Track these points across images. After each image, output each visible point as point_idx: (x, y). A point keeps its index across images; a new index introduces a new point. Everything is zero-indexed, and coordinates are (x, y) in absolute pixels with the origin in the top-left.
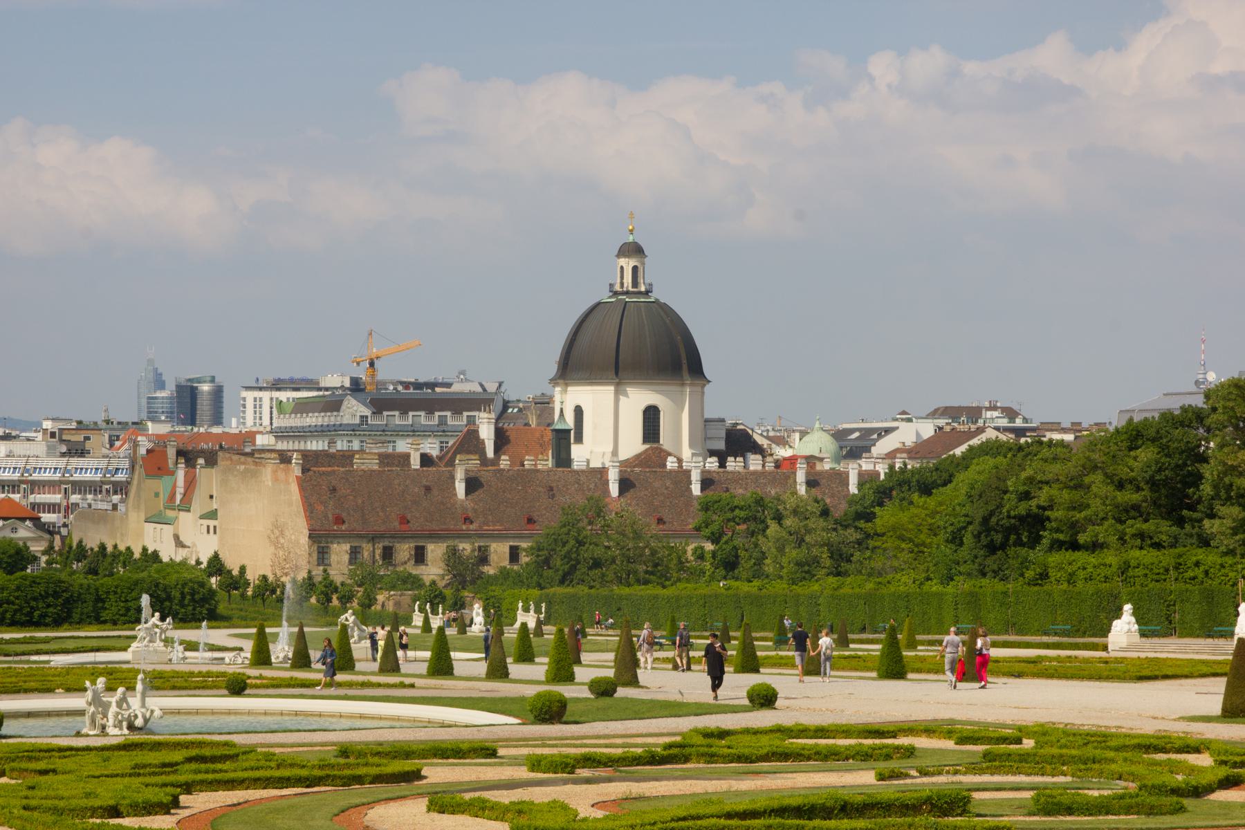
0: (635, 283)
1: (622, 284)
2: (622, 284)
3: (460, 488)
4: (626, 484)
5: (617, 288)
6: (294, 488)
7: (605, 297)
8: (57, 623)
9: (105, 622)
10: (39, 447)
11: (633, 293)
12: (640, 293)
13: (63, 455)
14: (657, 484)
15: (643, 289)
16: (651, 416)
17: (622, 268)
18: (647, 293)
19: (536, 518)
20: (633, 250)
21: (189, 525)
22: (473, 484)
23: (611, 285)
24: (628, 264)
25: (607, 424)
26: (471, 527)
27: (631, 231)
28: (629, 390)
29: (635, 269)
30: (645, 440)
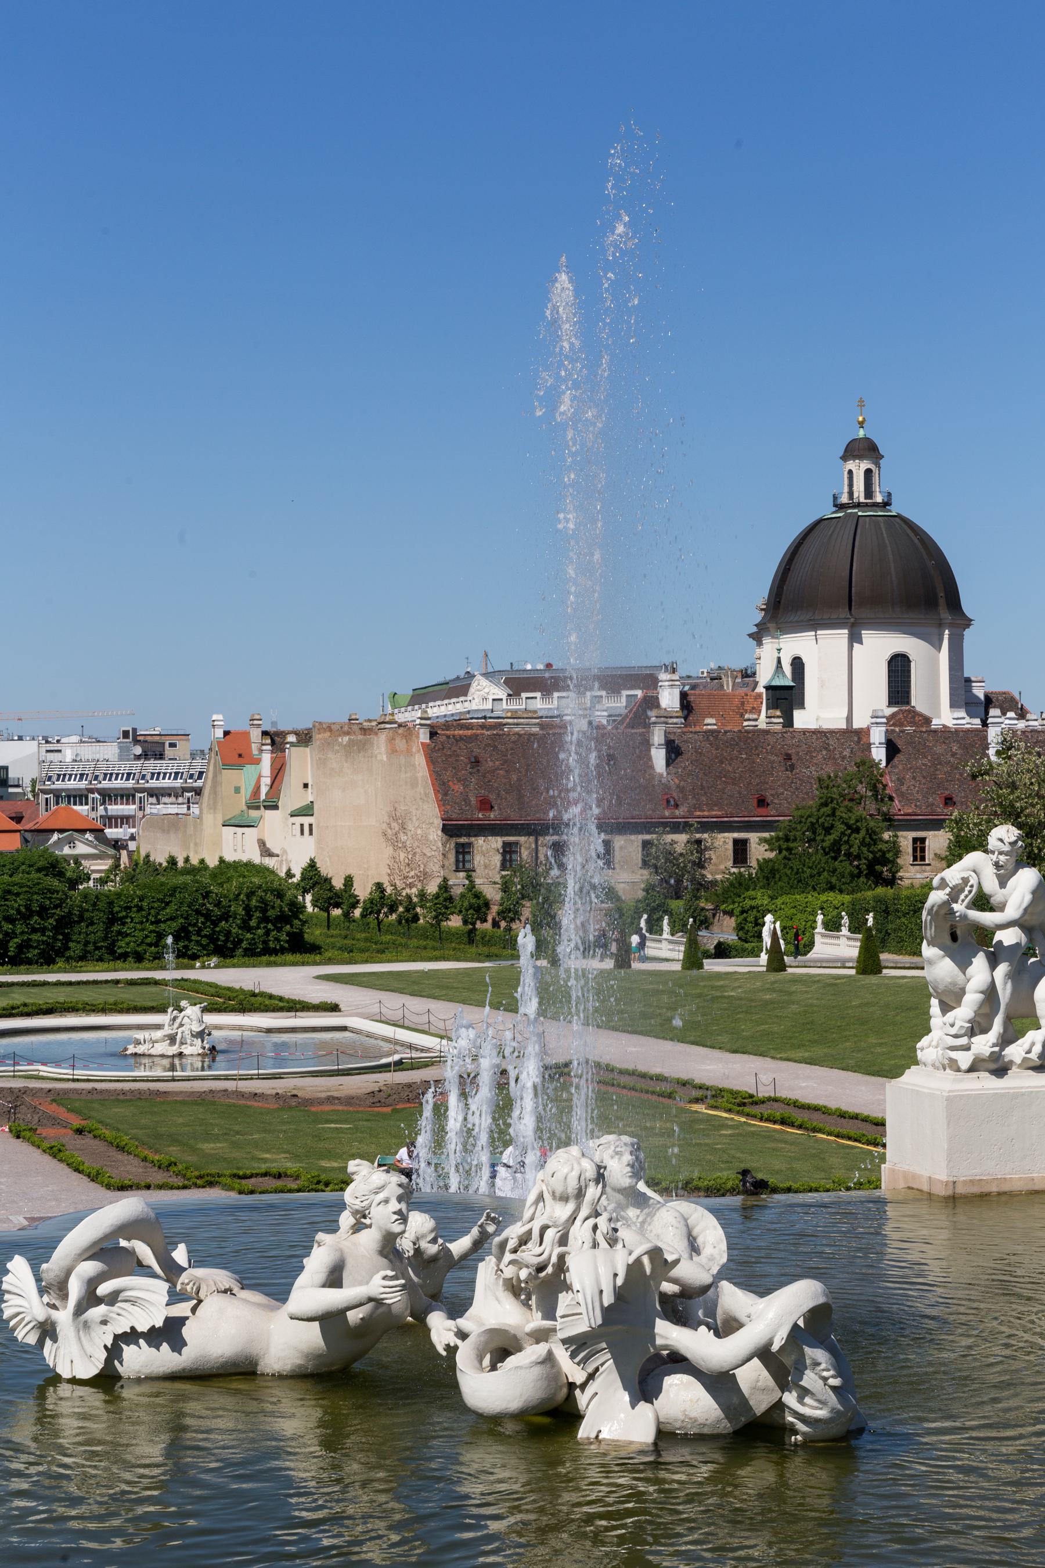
0: (869, 492)
1: (851, 494)
2: (851, 494)
3: (659, 757)
4: (892, 749)
5: (844, 499)
6: (420, 760)
7: (828, 511)
8: (48, 959)
9: (124, 957)
10: (110, 751)
11: (866, 505)
12: (875, 505)
13: (138, 758)
14: (939, 749)
15: (879, 498)
16: (899, 668)
17: (850, 472)
18: (886, 504)
19: (769, 799)
20: (863, 449)
21: (275, 827)
22: (673, 750)
23: (835, 498)
24: (859, 468)
25: (842, 680)
26: (677, 812)
27: (861, 424)
28: (866, 634)
29: (868, 473)
30: (891, 703)
